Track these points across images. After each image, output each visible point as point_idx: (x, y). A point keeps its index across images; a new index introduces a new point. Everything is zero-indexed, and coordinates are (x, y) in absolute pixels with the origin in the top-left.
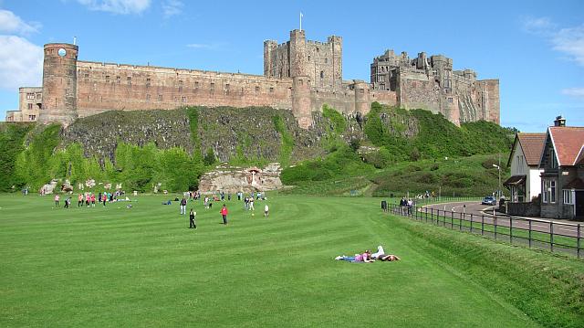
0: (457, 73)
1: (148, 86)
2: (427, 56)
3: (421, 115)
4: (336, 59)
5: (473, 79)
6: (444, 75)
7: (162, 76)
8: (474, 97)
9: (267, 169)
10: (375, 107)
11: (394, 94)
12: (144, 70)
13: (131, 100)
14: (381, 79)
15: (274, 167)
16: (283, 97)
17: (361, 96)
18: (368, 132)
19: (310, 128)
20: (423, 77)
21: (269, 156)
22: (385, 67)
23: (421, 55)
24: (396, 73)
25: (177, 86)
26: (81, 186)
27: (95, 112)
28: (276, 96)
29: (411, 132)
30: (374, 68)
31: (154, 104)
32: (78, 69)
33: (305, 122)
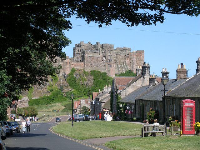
0: (118, 49)
2: (101, 43)
3: (94, 73)
5: (127, 52)
6: (108, 53)
8: (128, 61)
10: (73, 71)
20: (97, 55)
22: (79, 50)
23: (97, 43)
24: (84, 53)
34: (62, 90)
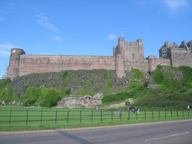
1: (48, 63)
2: (186, 42)
4: (140, 48)
7: (54, 59)
9: (95, 96)
10: (159, 67)
11: (169, 60)
12: (47, 56)
13: (41, 68)
14: (163, 55)
15: (99, 95)
16: (111, 64)
17: (151, 62)
18: (155, 78)
19: (123, 77)
20: (185, 51)
21: (97, 90)
23: (183, 43)
25: (61, 62)
26: (10, 103)
27: (26, 74)
28: (107, 64)
29: (179, 77)
30: (160, 51)
31: (50, 70)
32: (21, 57)
33: (121, 74)
34: (146, 86)
